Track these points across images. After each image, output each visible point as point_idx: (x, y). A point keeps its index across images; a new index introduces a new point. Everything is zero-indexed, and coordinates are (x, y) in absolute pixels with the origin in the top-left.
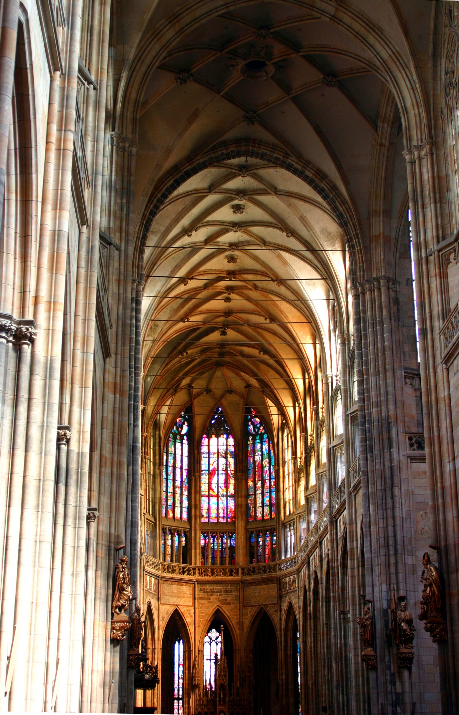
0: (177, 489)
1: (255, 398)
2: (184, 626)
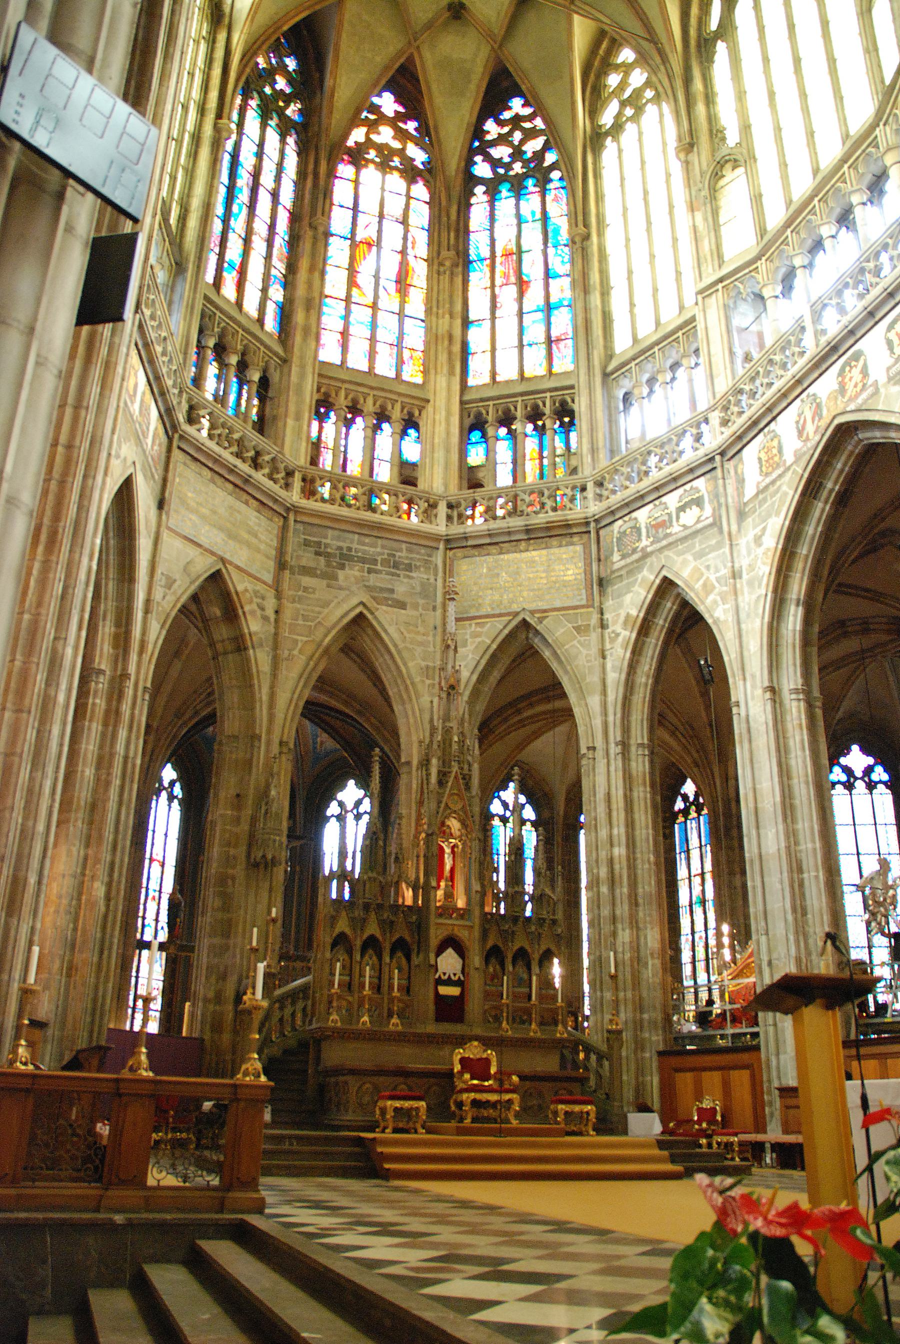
1: (523, 55)
2: (240, 645)
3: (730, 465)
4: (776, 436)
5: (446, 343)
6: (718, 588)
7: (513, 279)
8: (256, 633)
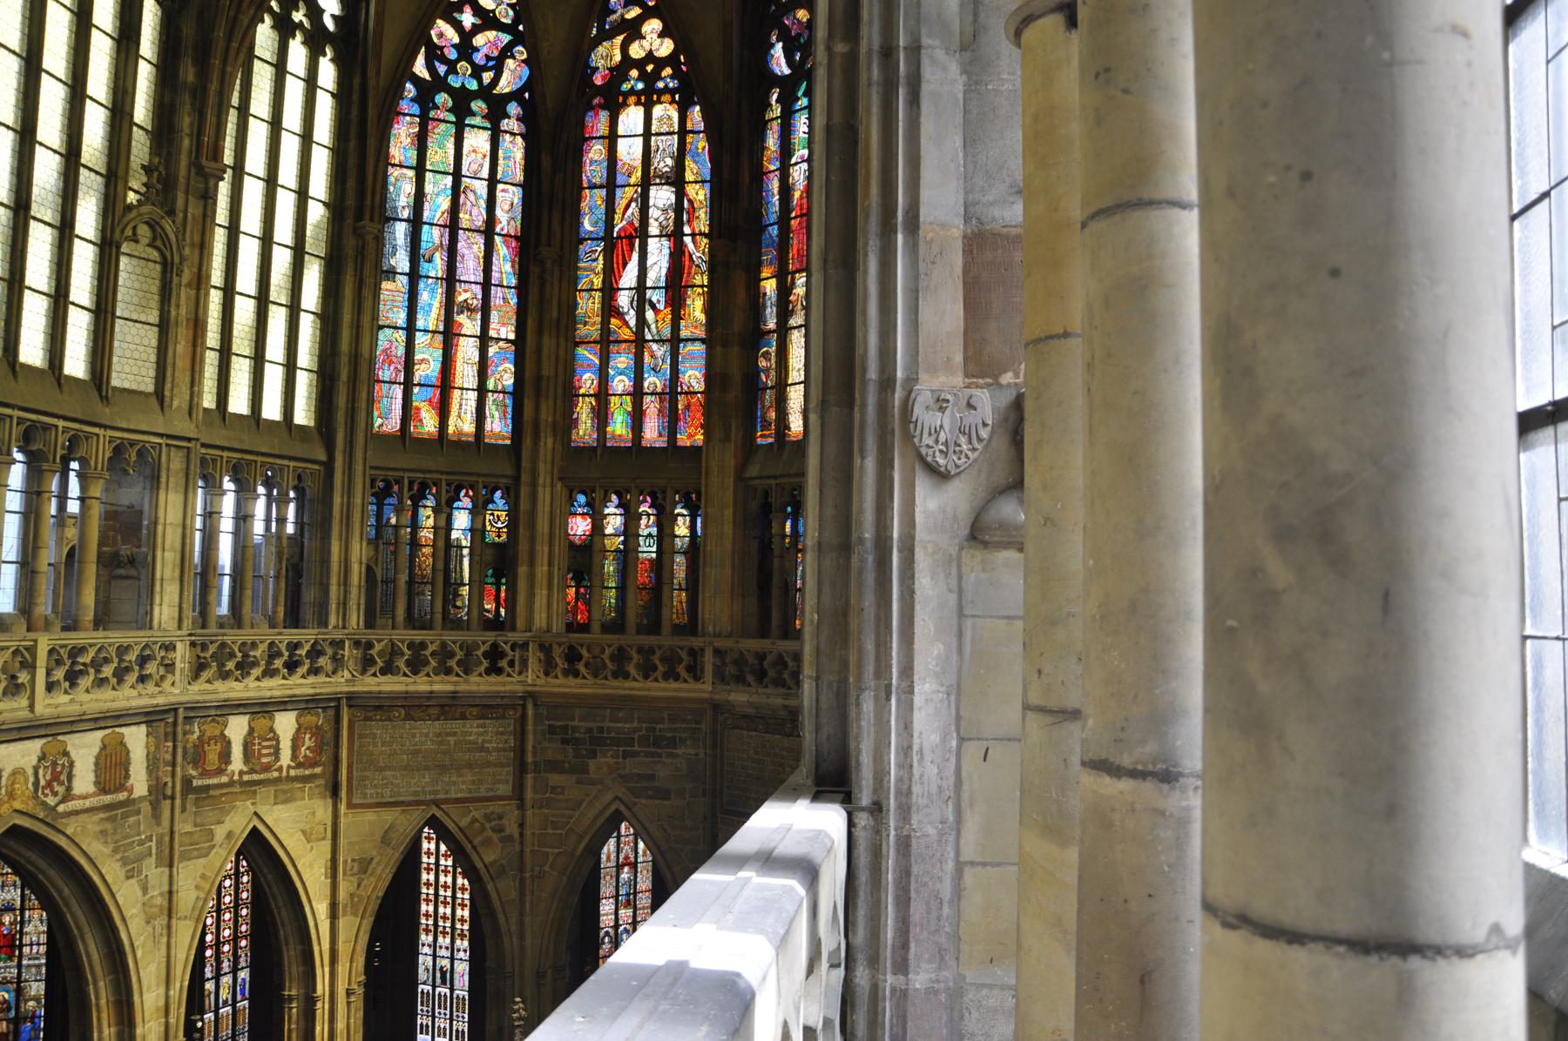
0: (461, 318)
8: (492, 864)
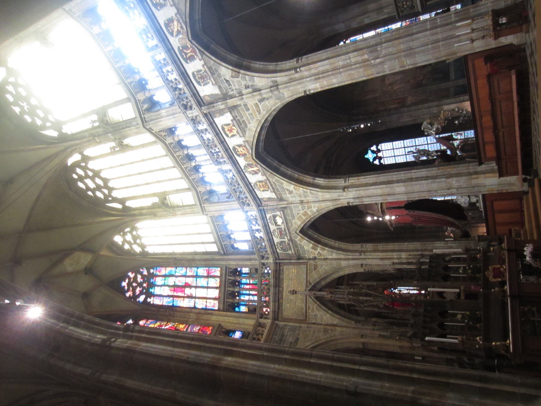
3: (264, 203)
4: (256, 183)
5: (200, 315)
6: (306, 210)
7: (183, 289)
